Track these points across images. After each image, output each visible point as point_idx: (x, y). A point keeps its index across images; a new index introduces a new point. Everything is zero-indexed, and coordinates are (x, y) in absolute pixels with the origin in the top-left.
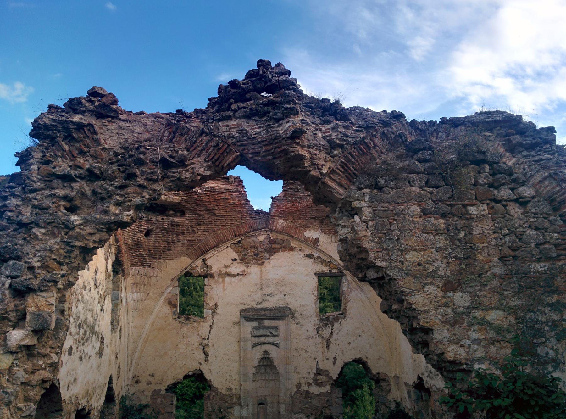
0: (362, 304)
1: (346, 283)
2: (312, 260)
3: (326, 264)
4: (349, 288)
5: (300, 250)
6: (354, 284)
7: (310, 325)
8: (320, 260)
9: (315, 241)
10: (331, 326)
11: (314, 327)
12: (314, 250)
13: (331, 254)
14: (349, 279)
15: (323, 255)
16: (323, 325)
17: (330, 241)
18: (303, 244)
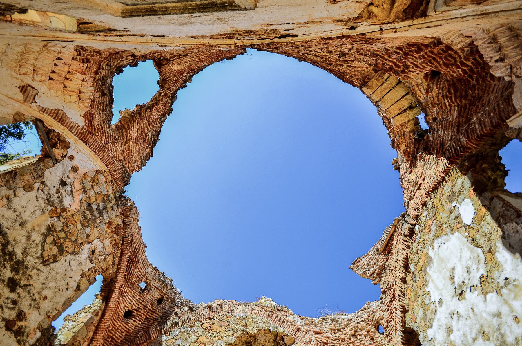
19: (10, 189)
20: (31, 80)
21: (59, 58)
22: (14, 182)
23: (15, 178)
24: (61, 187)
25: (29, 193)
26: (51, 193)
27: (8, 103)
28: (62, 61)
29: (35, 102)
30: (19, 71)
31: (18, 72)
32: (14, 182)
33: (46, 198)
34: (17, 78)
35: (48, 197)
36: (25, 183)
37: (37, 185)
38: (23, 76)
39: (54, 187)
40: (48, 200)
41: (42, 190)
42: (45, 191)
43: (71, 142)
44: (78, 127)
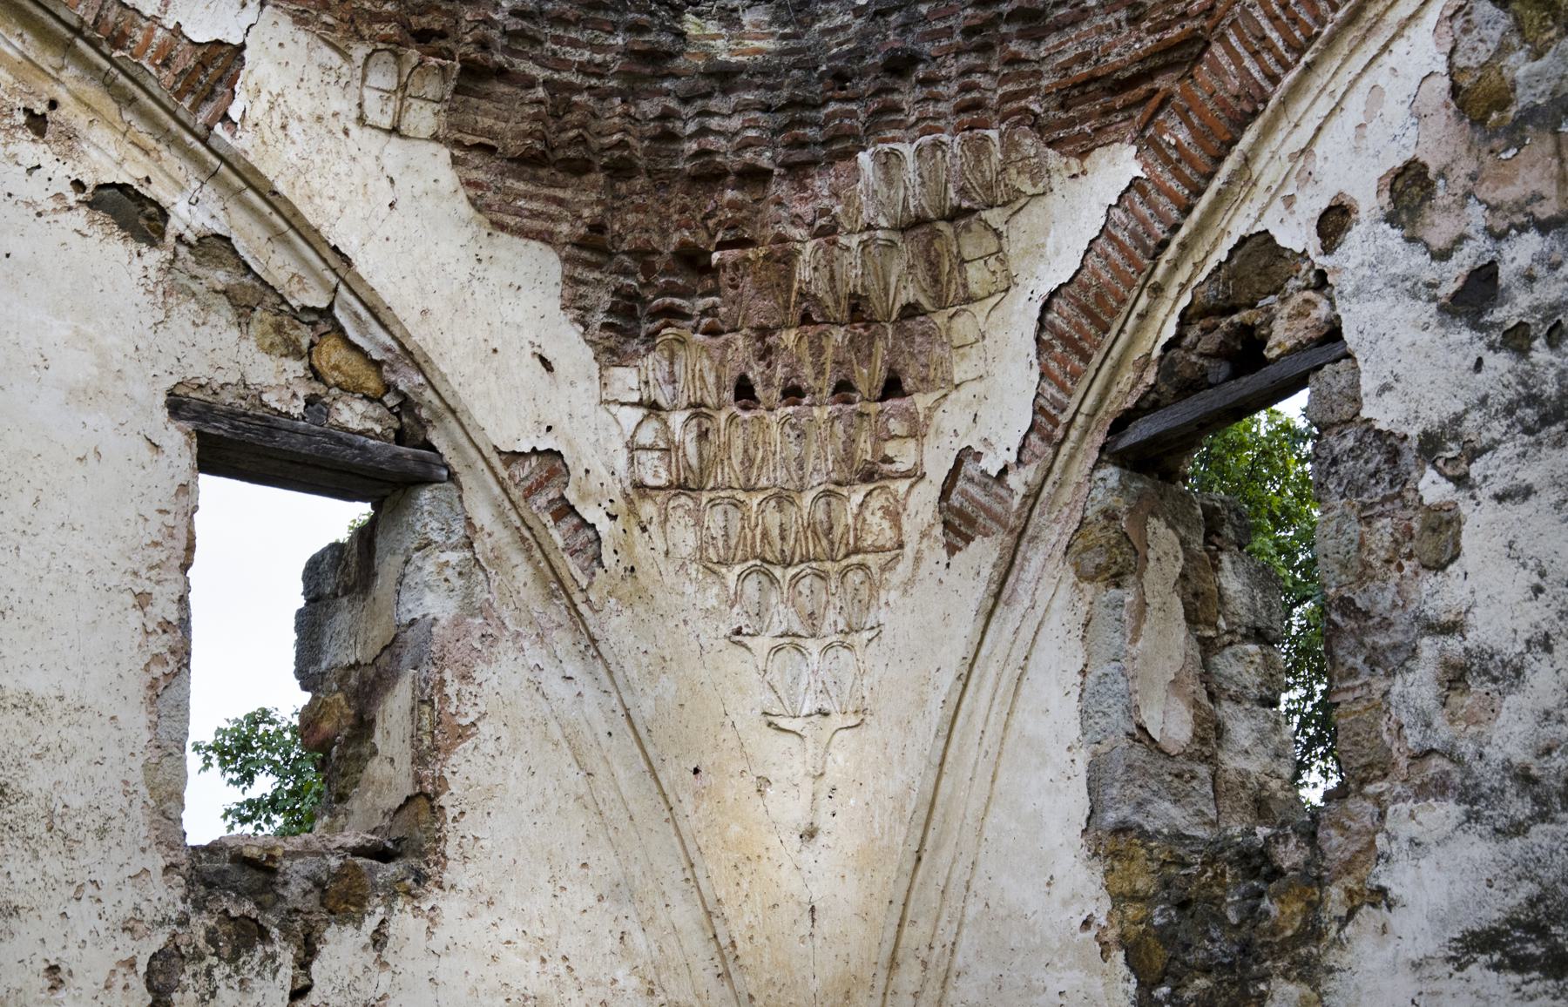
0: (573, 776)
1: (453, 557)
2: (154, 257)
3: (278, 329)
4: (470, 607)
5: (37, 124)
6: (523, 572)
7: (82, 914)
8: (220, 277)
9: (203, 65)
10: (287, 956)
11: (126, 946)
12: (173, 160)
13: (342, 235)
14: (483, 515)
15: (258, 232)
16: (211, 938)
17: (344, 105)
18: (70, 73)
19: (1414, 653)
20: (921, 486)
21: (744, 391)
22: (1386, 624)
23: (1367, 615)
24: (1498, 314)
25: (1465, 541)
26: (1510, 394)
27: (1027, 603)
28: (755, 374)
29: (1004, 471)
30: (881, 549)
31: (889, 556)
32: (1386, 624)
33: (1528, 431)
34: (918, 560)
35: (1529, 414)
36: (1410, 556)
37: (1433, 487)
38: (907, 526)
39: (1479, 365)
40: (1545, 421)
41: (1474, 454)
42: (1486, 437)
43: (1240, 224)
44: (1144, 193)
